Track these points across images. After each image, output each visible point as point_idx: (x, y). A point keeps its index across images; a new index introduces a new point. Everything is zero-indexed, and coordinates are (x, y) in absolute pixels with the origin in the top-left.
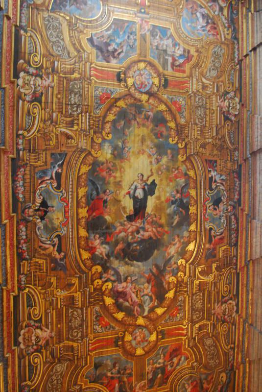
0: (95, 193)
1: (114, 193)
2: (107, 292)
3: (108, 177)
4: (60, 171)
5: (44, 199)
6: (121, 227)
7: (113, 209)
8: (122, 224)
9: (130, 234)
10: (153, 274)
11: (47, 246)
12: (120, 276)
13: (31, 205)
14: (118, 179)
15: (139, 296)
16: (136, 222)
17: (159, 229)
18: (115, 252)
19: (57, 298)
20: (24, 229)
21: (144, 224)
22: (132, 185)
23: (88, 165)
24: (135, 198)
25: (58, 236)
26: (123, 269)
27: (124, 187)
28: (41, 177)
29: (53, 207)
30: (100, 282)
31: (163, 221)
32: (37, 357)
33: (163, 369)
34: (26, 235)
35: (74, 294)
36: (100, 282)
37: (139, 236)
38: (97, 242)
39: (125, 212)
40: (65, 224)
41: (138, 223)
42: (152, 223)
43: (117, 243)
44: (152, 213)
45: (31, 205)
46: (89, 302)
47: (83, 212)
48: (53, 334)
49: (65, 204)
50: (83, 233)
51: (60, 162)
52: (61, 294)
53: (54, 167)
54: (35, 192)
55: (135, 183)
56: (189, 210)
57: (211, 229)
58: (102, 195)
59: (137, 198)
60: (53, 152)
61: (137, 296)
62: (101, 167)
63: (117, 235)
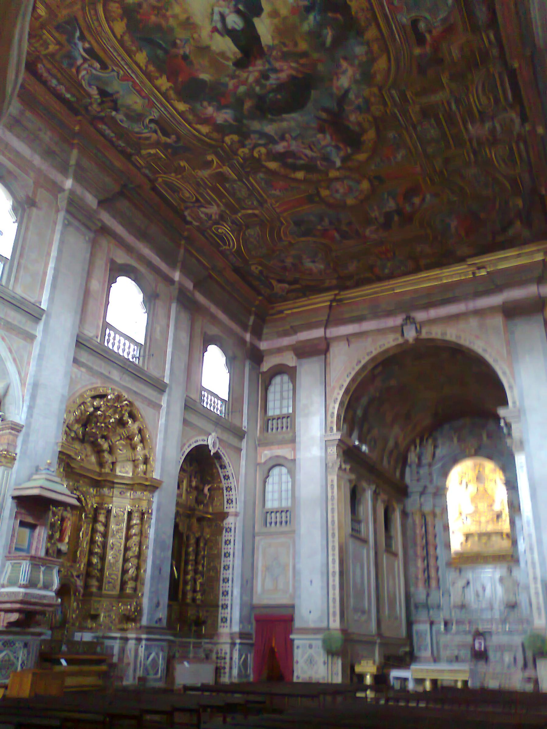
0: (159, 52)
1: (191, 40)
2: (263, 157)
3: (163, 23)
4: (87, 45)
5: (98, 88)
6: (234, 81)
7: (206, 62)
8: (232, 77)
9: (254, 85)
10: (324, 121)
11: (148, 135)
12: (273, 137)
13: (89, 101)
14: (183, 17)
15: (315, 149)
16: (254, 65)
17: (303, 61)
18: (245, 112)
19: (202, 179)
20: (104, 127)
21: (269, 63)
22: (212, 14)
23: (119, 19)
24: (231, 33)
25: (151, 121)
26: (270, 129)
27: (200, 23)
28: (71, 65)
29: (117, 92)
30: (246, 150)
31: (303, 46)
32: (219, 228)
33: (399, 211)
34: (113, 132)
35: (220, 170)
36: (246, 150)
37: (272, 81)
38: (210, 110)
39: (228, 59)
40: (152, 105)
41: (259, 65)
42: (285, 57)
43: (240, 102)
44: (276, 42)
45: (89, 101)
46: (246, 172)
47: (163, 82)
48: (223, 208)
49: (130, 83)
50: (182, 107)
51: (78, 34)
52: (205, 173)
53: (75, 44)
54: (81, 86)
55: (216, 10)
56: (348, 8)
57: (415, 23)
58: (174, 51)
59: (234, 30)
60: (55, 23)
61: (311, 149)
62: (141, 11)
63: (235, 93)
